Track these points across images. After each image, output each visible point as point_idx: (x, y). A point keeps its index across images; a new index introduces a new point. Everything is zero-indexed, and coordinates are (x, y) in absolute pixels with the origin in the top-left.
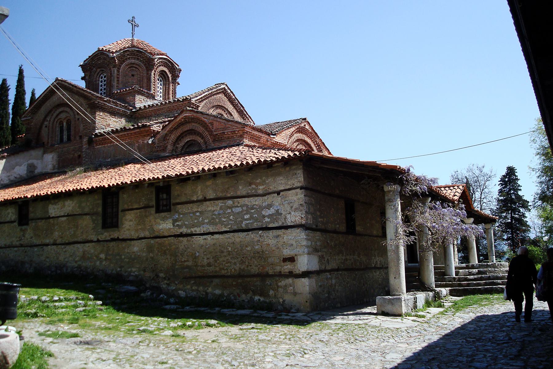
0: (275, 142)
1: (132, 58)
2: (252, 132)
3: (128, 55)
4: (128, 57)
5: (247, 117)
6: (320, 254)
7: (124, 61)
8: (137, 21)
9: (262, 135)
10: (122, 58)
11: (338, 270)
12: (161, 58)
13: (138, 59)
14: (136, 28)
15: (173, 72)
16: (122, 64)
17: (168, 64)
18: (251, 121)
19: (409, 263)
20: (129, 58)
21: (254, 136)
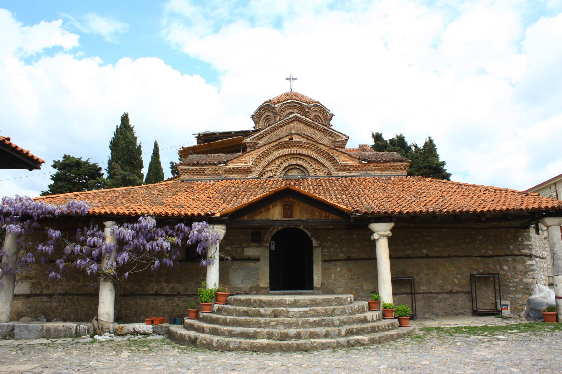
0: (228, 169)
1: (266, 112)
2: (189, 168)
3: (263, 110)
4: (264, 112)
5: (335, 134)
6: (33, 281)
7: (262, 116)
8: (289, 76)
9: (205, 167)
10: (260, 115)
11: (66, 294)
12: (285, 104)
13: (270, 111)
14: (294, 82)
15: (303, 110)
16: (260, 119)
17: (297, 106)
18: (342, 136)
19: (271, 290)
20: (264, 113)
21: (199, 171)
